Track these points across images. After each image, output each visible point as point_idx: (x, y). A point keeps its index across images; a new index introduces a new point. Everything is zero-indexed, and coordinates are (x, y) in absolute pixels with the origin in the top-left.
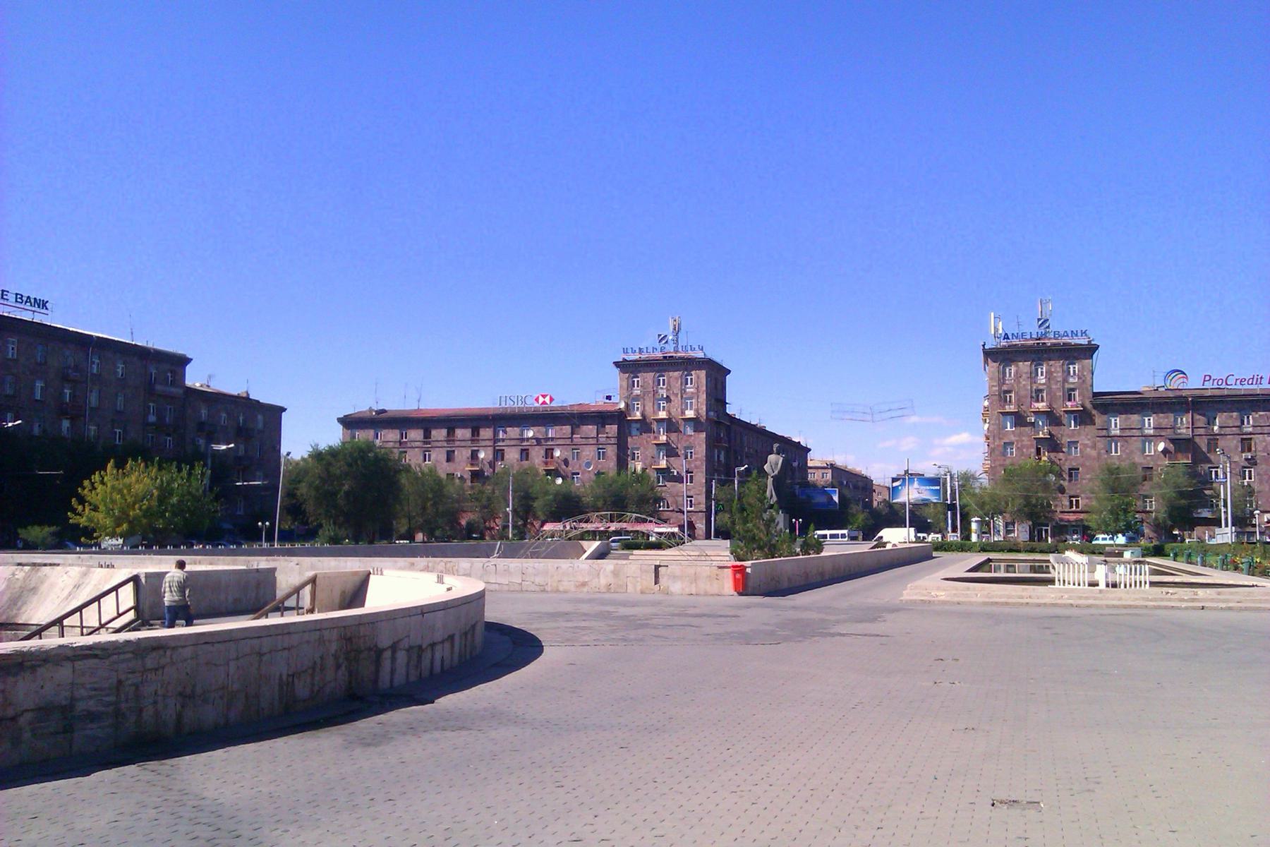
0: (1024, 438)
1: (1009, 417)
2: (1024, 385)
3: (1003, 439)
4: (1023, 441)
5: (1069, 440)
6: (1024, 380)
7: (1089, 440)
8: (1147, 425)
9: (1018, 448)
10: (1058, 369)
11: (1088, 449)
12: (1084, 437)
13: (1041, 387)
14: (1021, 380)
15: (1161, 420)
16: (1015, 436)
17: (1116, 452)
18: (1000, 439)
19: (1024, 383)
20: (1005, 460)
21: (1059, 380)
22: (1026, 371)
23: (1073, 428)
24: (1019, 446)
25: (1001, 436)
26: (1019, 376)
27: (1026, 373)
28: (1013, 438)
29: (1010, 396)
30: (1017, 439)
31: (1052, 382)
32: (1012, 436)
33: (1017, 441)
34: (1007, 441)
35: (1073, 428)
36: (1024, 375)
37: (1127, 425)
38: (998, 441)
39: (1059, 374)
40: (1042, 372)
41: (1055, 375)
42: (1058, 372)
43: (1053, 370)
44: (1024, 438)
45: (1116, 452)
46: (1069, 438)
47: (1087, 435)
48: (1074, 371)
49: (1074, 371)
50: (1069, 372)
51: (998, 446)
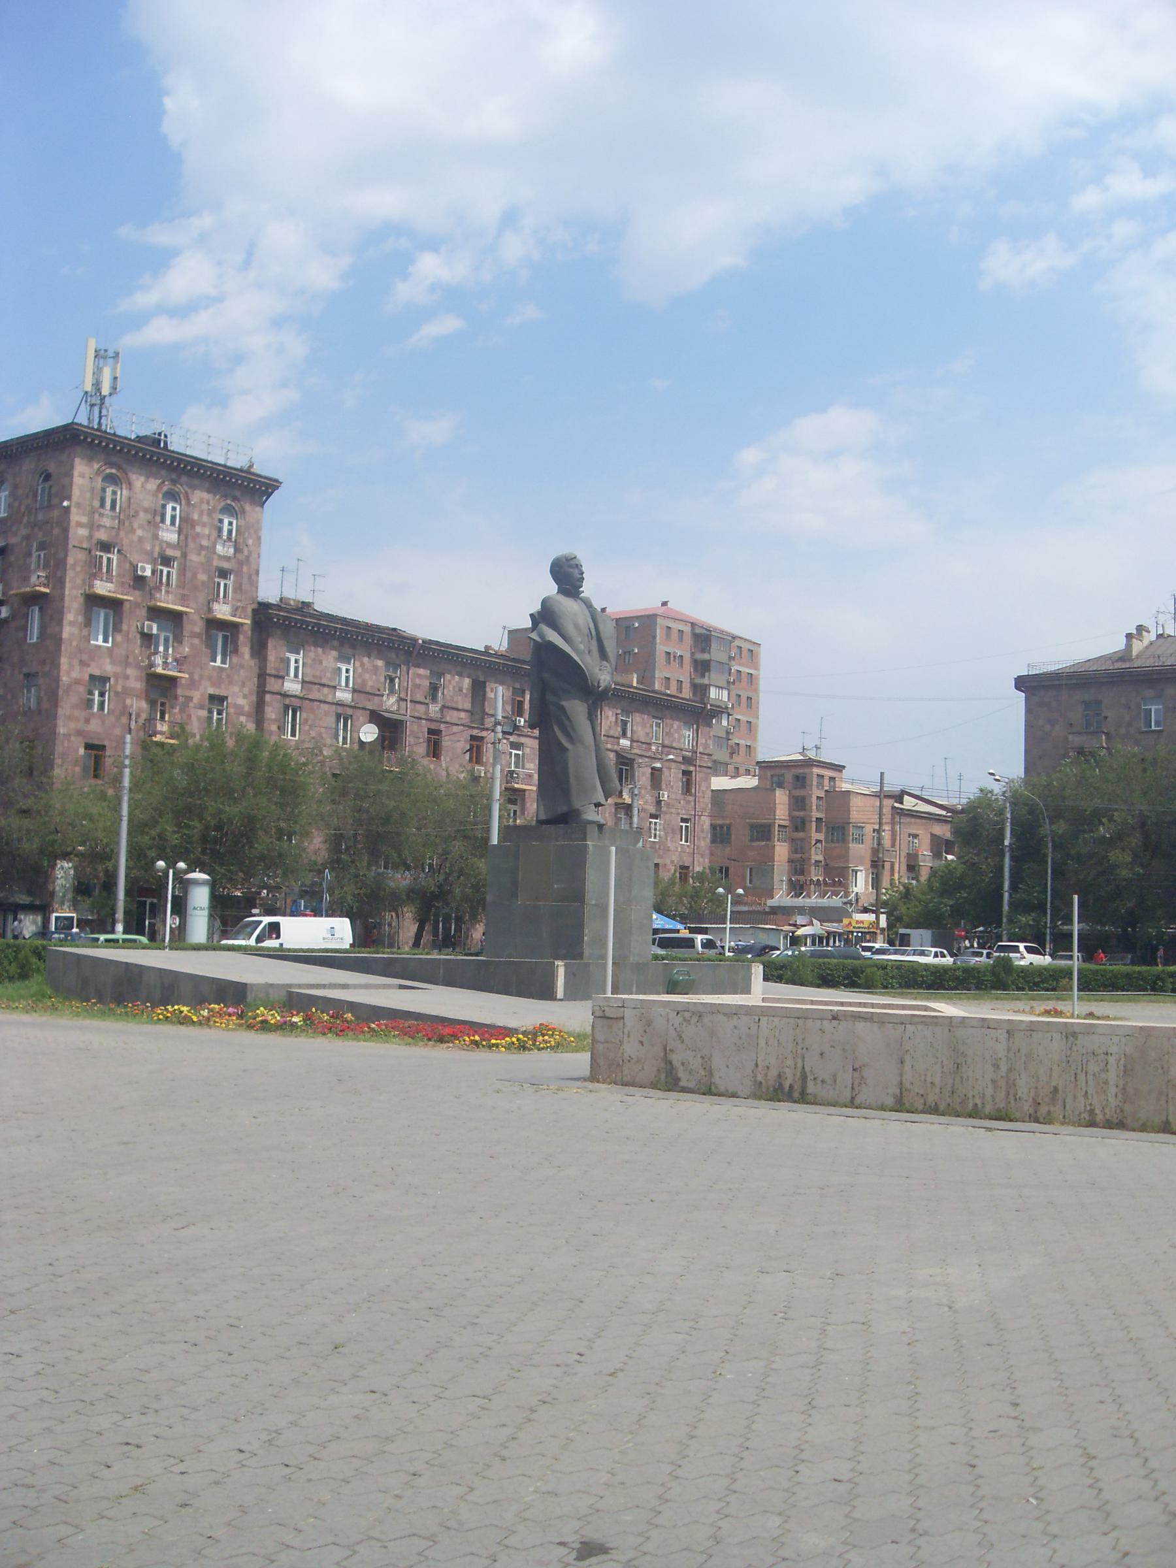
0: (129, 671)
1: (102, 613)
2: (141, 539)
3: (88, 665)
4: (127, 677)
5: (211, 691)
6: (141, 527)
7: (245, 697)
8: (343, 684)
9: (117, 693)
10: (205, 519)
11: (243, 719)
12: (236, 689)
13: (170, 552)
14: (136, 525)
15: (367, 676)
16: (113, 663)
17: (293, 734)
18: (83, 664)
19: (139, 532)
20: (87, 721)
21: (205, 543)
22: (146, 504)
23: (218, 663)
24: (119, 689)
25: (85, 657)
26: (132, 513)
27: (146, 510)
28: (109, 668)
29: (109, 559)
30: (118, 670)
31: (191, 545)
32: (108, 660)
33: (117, 676)
34: (97, 673)
35: (218, 663)
36: (142, 515)
37: (314, 676)
38: (77, 668)
39: (207, 531)
40: (173, 518)
41: (198, 529)
42: (204, 525)
43: (196, 517)
44: (129, 671)
45: (293, 734)
46: (214, 685)
47: (243, 685)
48: (230, 532)
49: (230, 532)
50: (220, 530)
51: (77, 682)
